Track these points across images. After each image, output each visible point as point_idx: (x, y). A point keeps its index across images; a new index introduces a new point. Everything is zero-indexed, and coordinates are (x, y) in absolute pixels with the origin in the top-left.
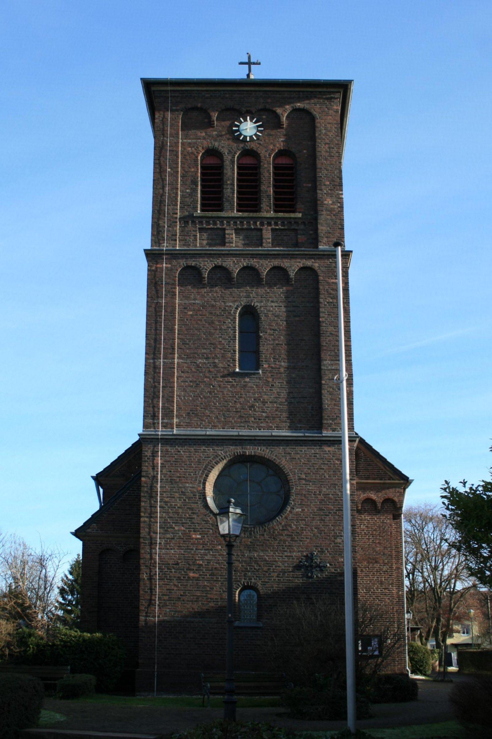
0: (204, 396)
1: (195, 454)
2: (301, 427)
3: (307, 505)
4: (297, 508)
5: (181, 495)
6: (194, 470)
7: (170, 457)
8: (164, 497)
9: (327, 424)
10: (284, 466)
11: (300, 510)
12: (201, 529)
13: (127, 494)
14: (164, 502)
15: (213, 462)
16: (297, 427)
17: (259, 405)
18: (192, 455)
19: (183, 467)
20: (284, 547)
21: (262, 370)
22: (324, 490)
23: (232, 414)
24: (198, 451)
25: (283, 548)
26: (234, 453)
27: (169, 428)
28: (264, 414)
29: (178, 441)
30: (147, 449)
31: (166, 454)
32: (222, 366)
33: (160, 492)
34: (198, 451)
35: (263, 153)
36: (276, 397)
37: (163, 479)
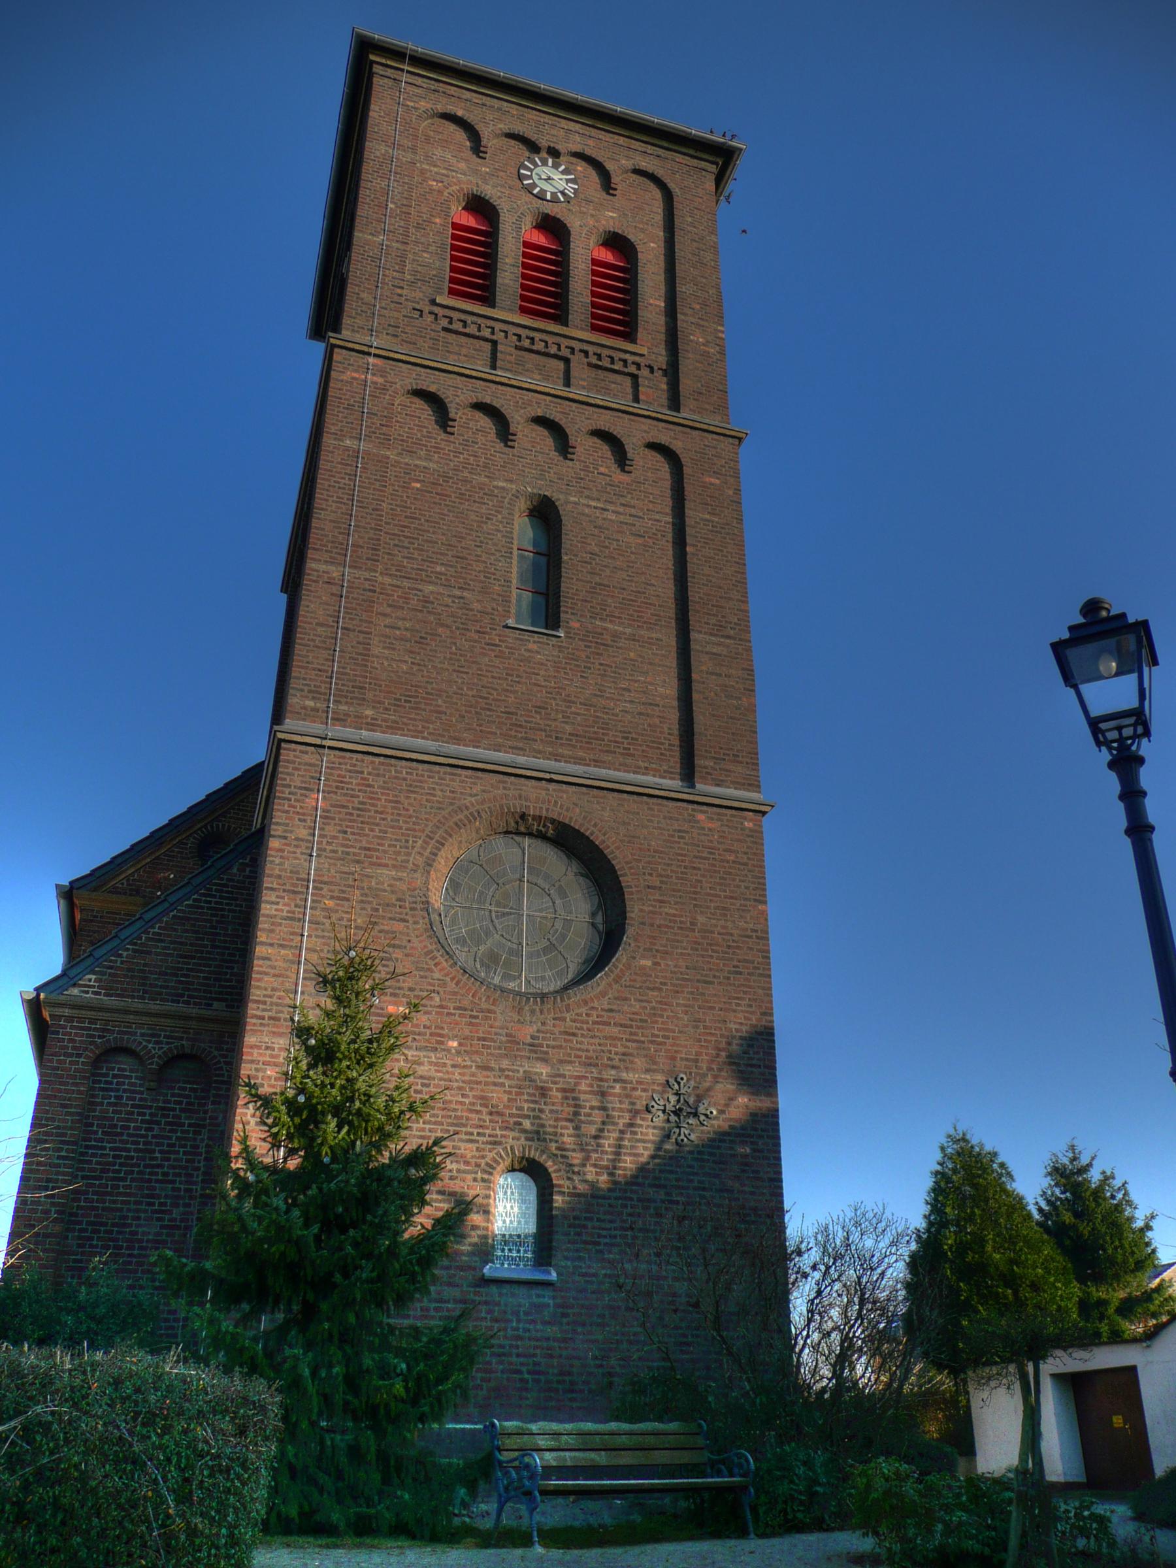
0: (434, 667)
1: (408, 797)
2: (646, 768)
3: (666, 953)
4: (643, 957)
5: (366, 895)
6: (403, 834)
7: (345, 795)
8: (323, 896)
9: (706, 767)
10: (613, 852)
11: (649, 963)
12: (410, 989)
13: (191, 902)
14: (324, 909)
15: (451, 824)
16: (639, 767)
17: (557, 705)
18: (402, 799)
19: (377, 825)
20: (613, 1056)
21: (566, 632)
22: (701, 919)
23: (498, 717)
24: (417, 790)
25: (609, 1059)
26: (502, 807)
27: (350, 727)
28: (568, 728)
29: (371, 758)
30: (290, 770)
31: (337, 787)
32: (479, 607)
33: (314, 881)
34: (417, 790)
35: (574, 223)
36: (596, 695)
37: (325, 850)
